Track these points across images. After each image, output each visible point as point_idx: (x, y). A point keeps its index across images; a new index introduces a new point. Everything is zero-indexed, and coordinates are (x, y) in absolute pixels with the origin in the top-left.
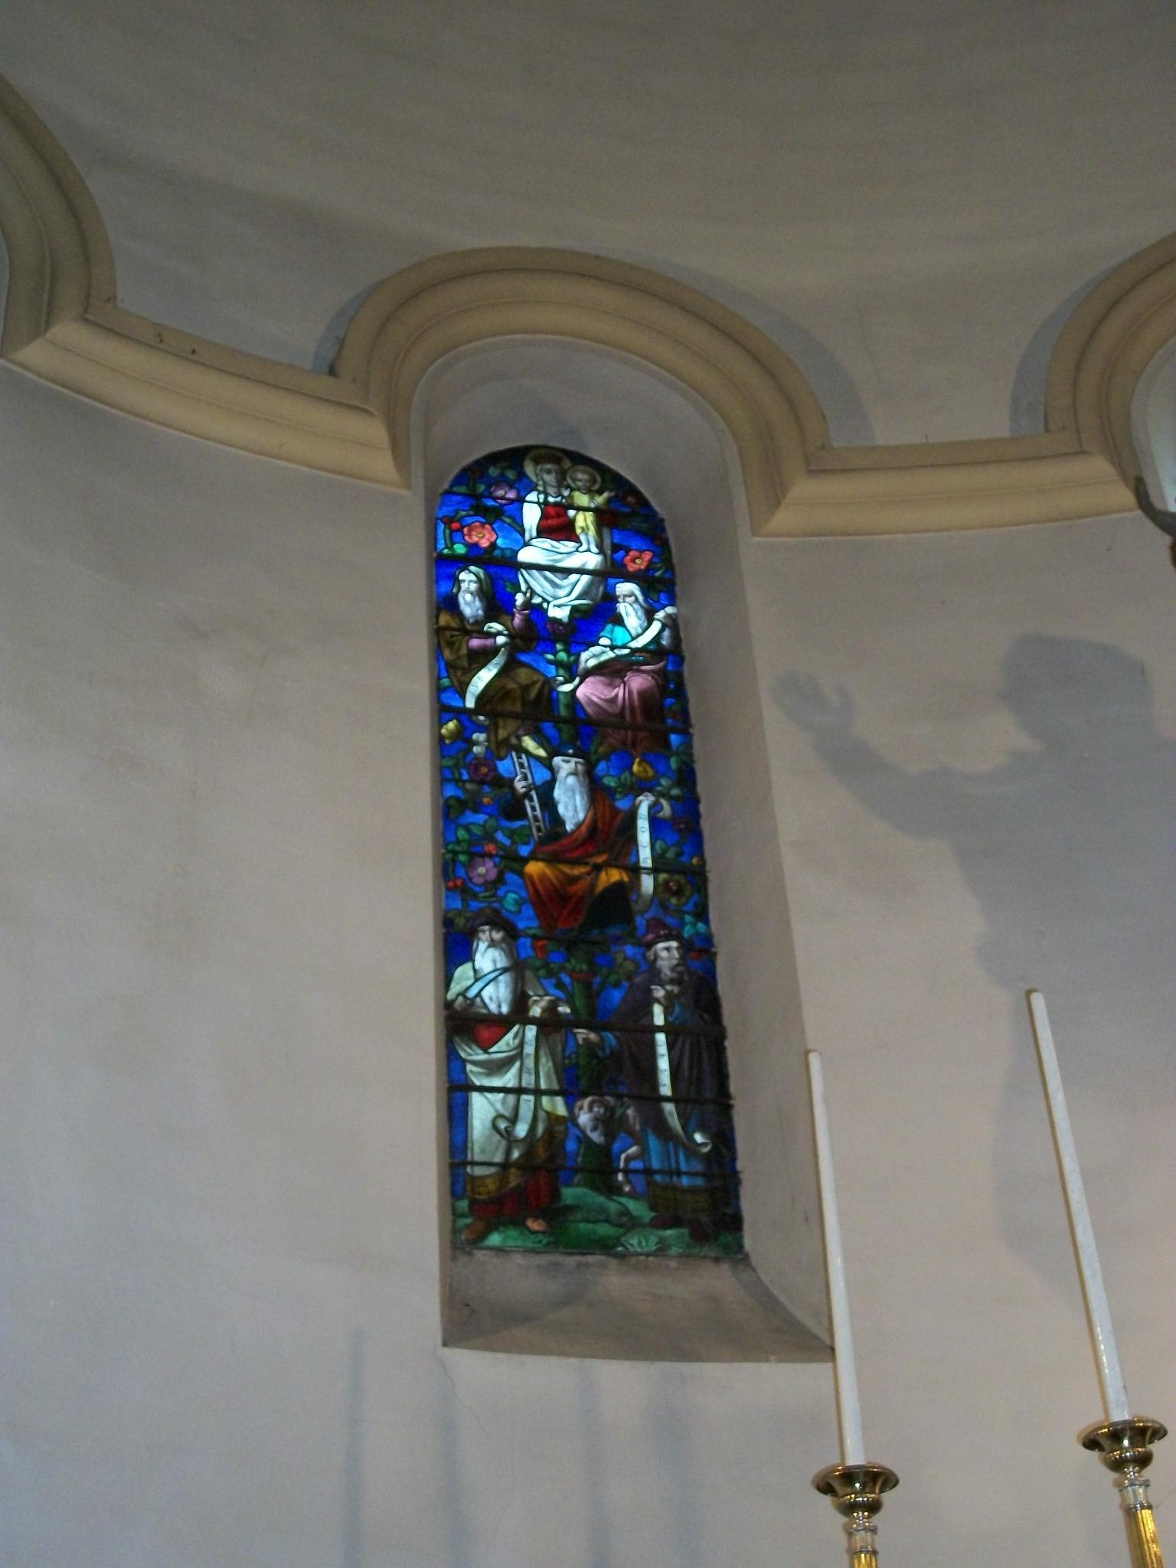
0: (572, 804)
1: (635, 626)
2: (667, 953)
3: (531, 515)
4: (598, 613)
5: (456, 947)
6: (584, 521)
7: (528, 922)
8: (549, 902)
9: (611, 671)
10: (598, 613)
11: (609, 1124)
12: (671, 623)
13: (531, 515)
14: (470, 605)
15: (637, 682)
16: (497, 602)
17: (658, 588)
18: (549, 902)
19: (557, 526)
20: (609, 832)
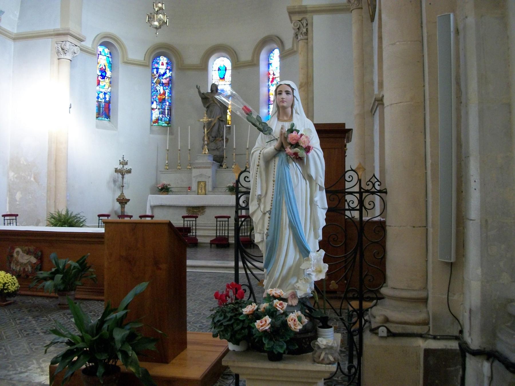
0: (162, 92)
1: (168, 74)
2: (167, 103)
3: (160, 63)
4: (165, 73)
5: (152, 103)
6: (165, 64)
7: (158, 101)
8: (159, 99)
9: (166, 79)
10: (165, 73)
11: (162, 117)
12: (171, 74)
13: (160, 63)
14: (155, 73)
15: (168, 79)
16: (157, 72)
17: (170, 70)
18: (159, 99)
19: (163, 64)
20: (164, 94)
